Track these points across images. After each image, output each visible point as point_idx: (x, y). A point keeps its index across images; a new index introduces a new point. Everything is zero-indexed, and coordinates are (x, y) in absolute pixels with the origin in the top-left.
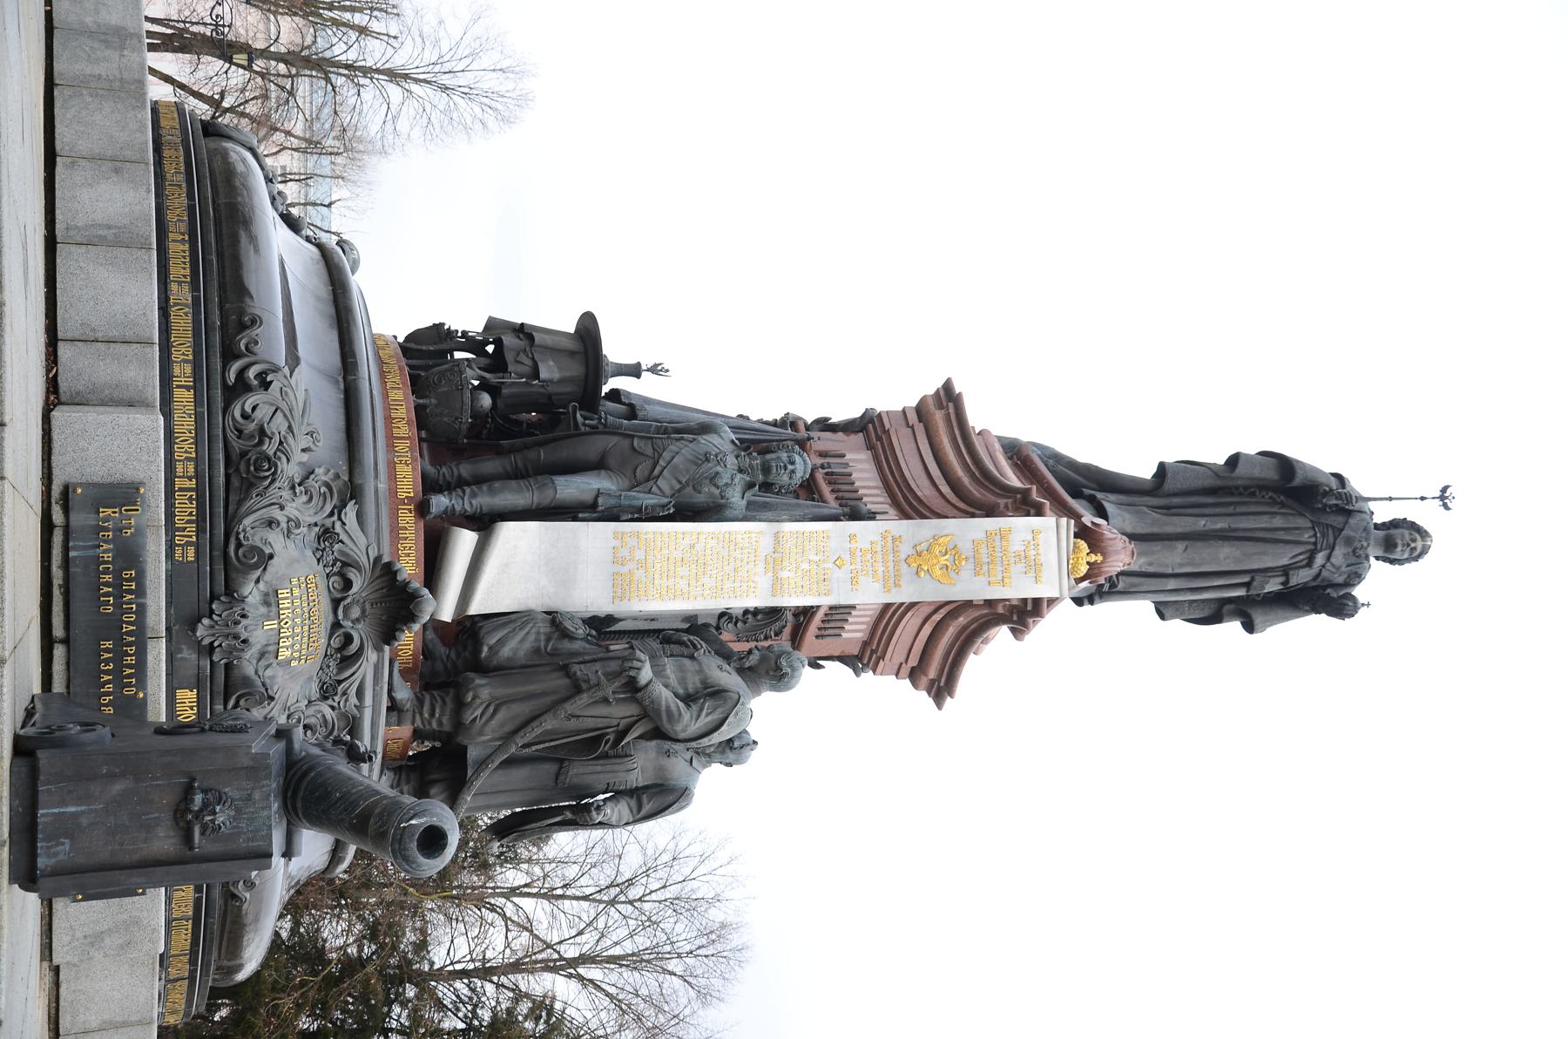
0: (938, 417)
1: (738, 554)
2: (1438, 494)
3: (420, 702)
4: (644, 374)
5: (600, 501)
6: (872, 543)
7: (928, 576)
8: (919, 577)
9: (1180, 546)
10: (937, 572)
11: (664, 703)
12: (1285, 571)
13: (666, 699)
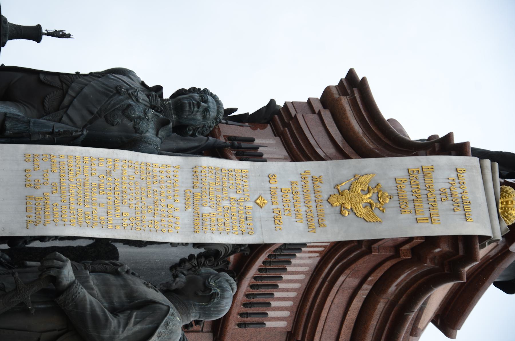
0: (345, 102)
1: (155, 187)
4: (44, 37)
5: (8, 125)
6: (292, 183)
7: (352, 215)
8: (343, 216)
10: (362, 211)
11: (88, 306)
13: (91, 302)
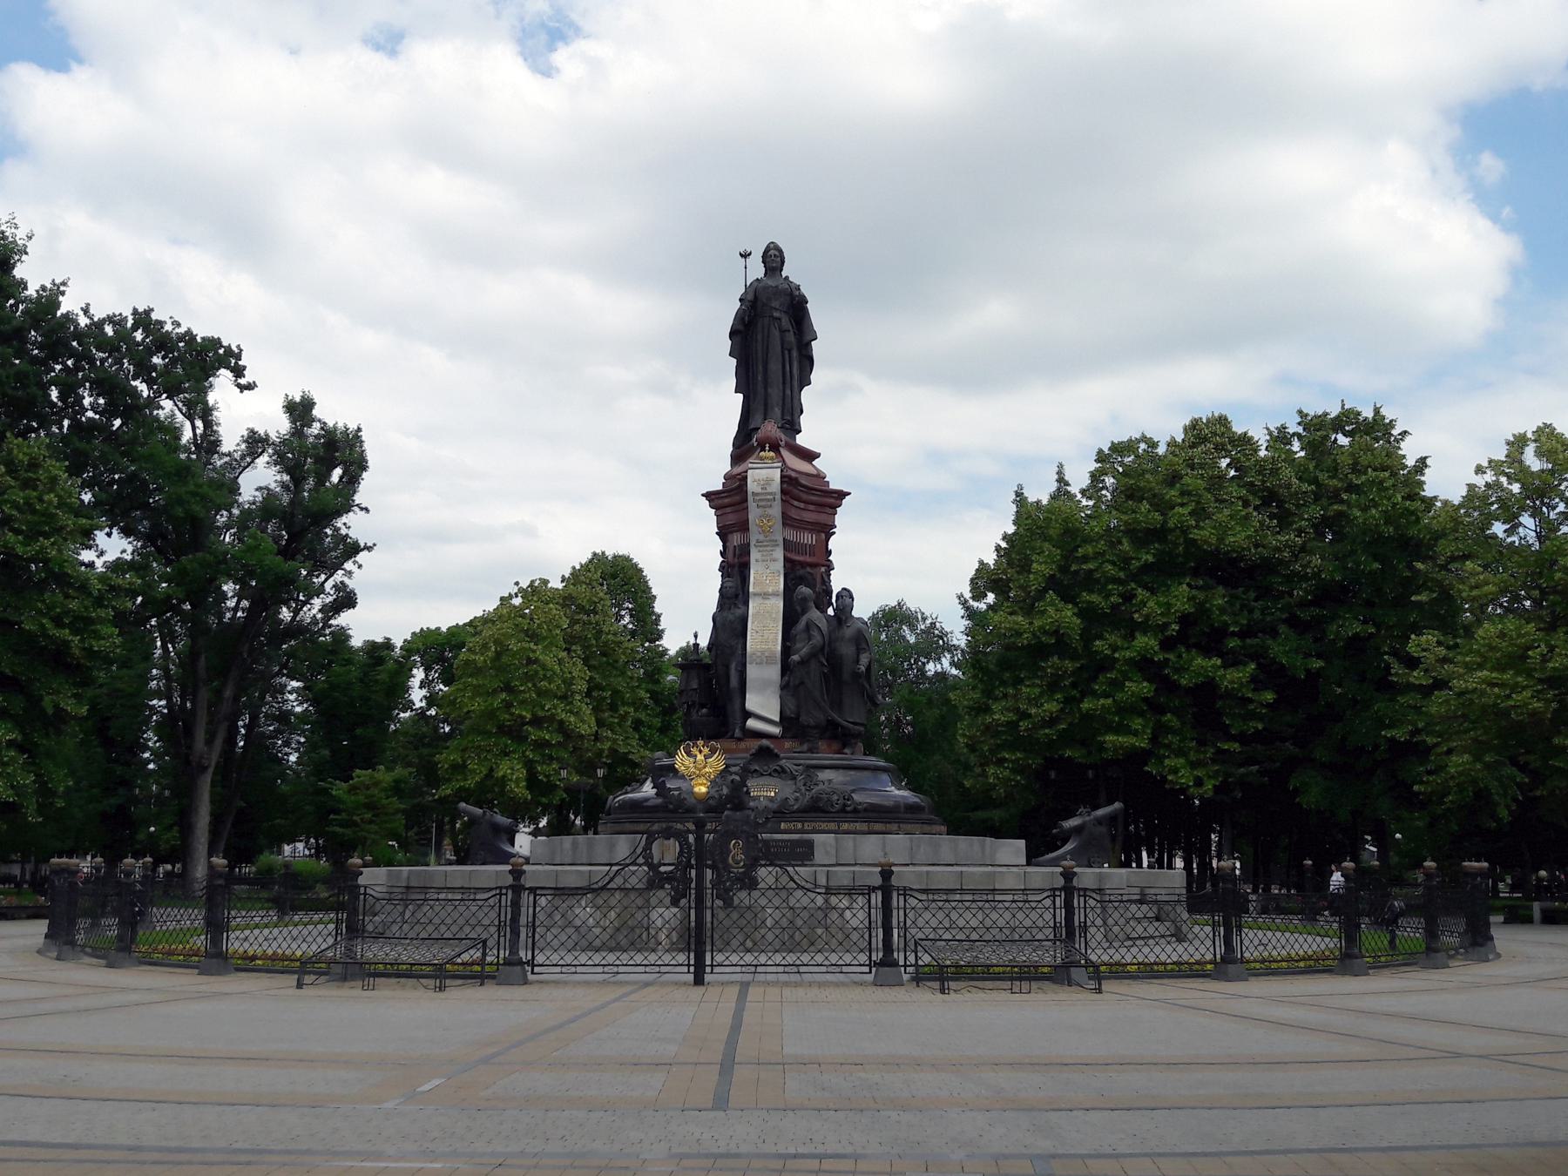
2: (744, 259)
3: (808, 741)
5: (739, 669)
9: (770, 390)
12: (783, 332)
